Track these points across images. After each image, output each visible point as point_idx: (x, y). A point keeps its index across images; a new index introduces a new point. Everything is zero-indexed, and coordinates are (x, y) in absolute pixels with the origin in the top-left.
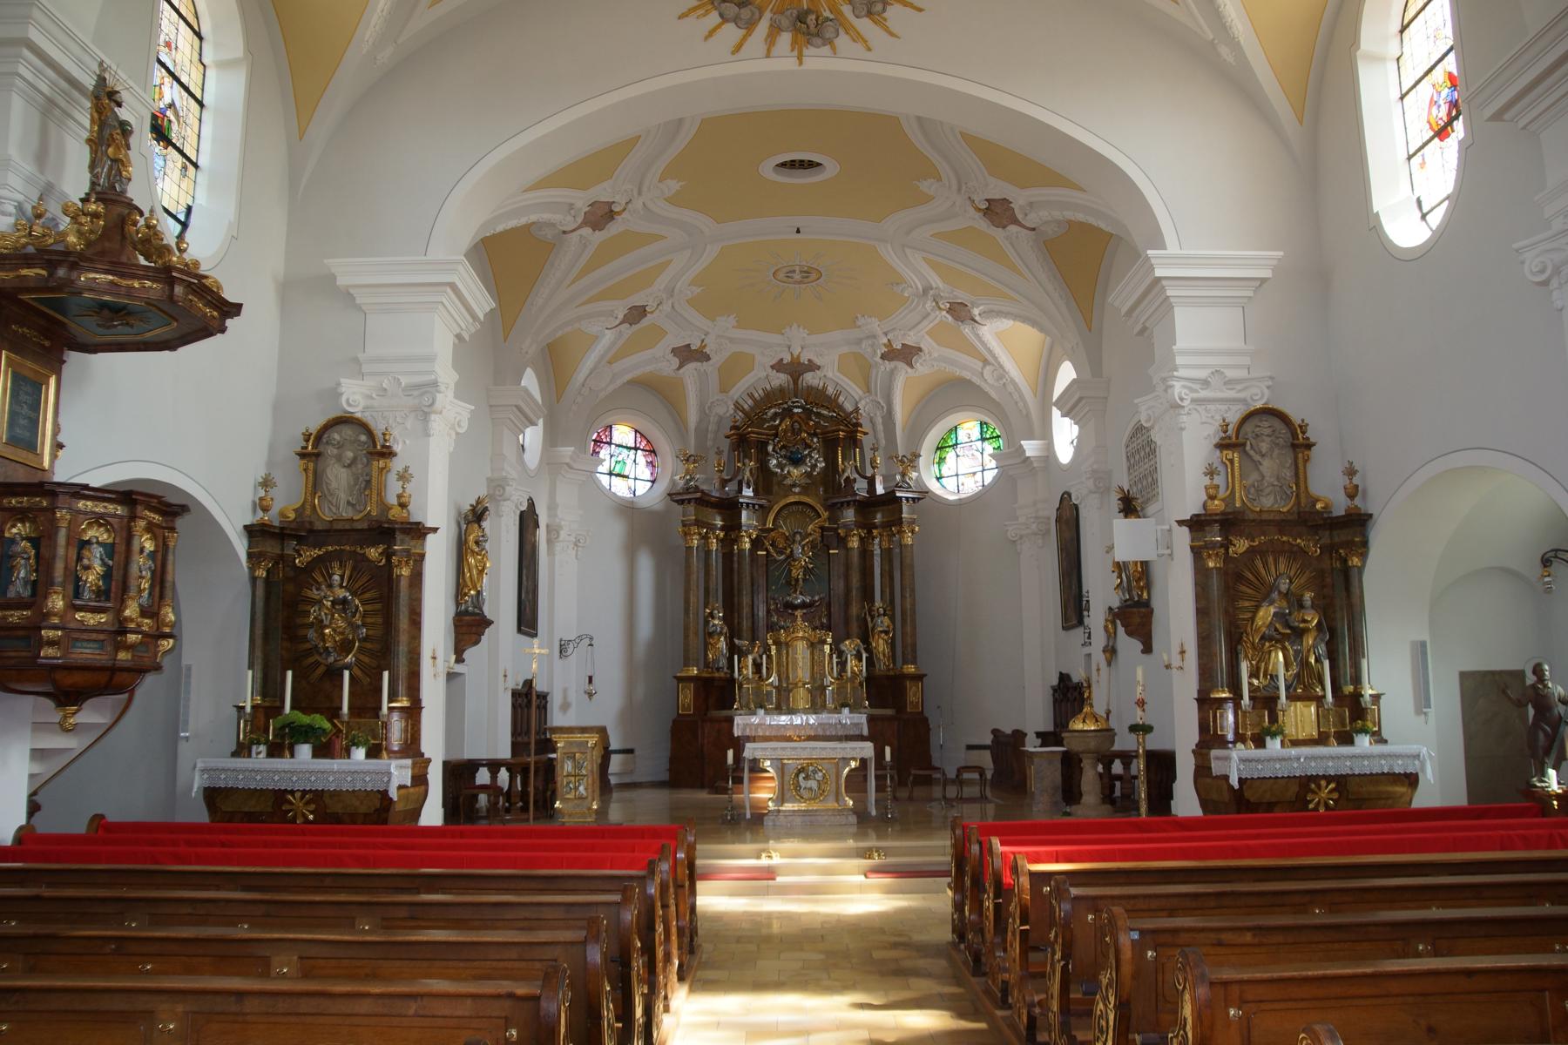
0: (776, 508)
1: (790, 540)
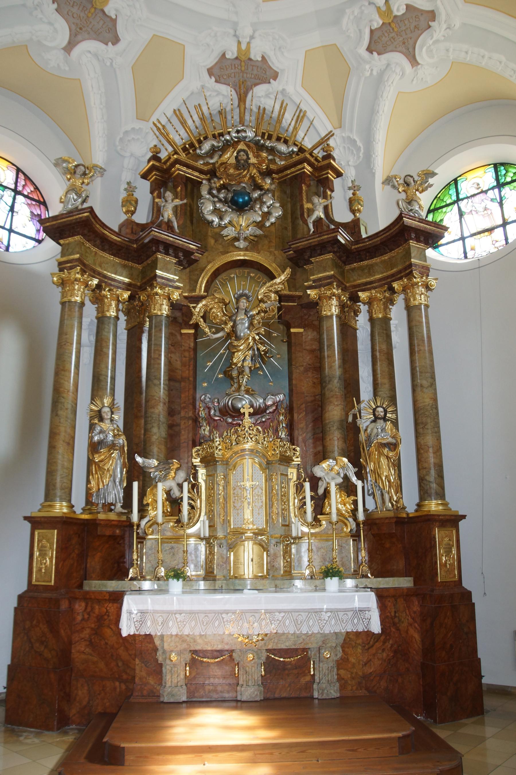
0: (211, 268)
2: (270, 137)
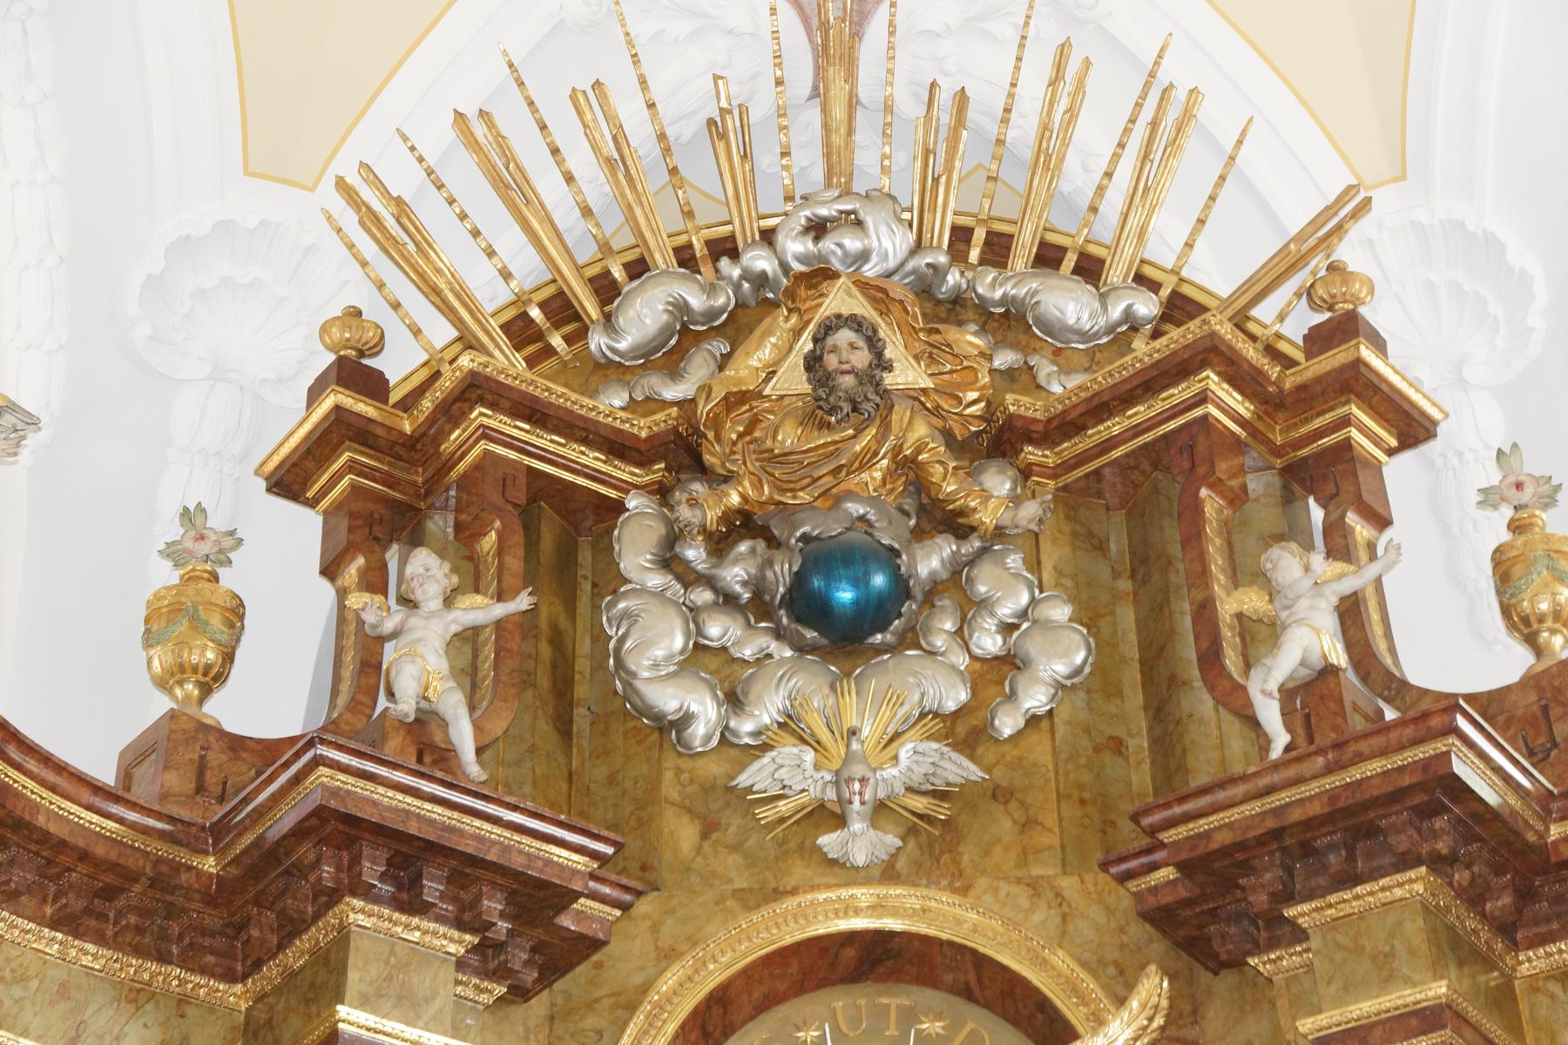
2: (998, 250)
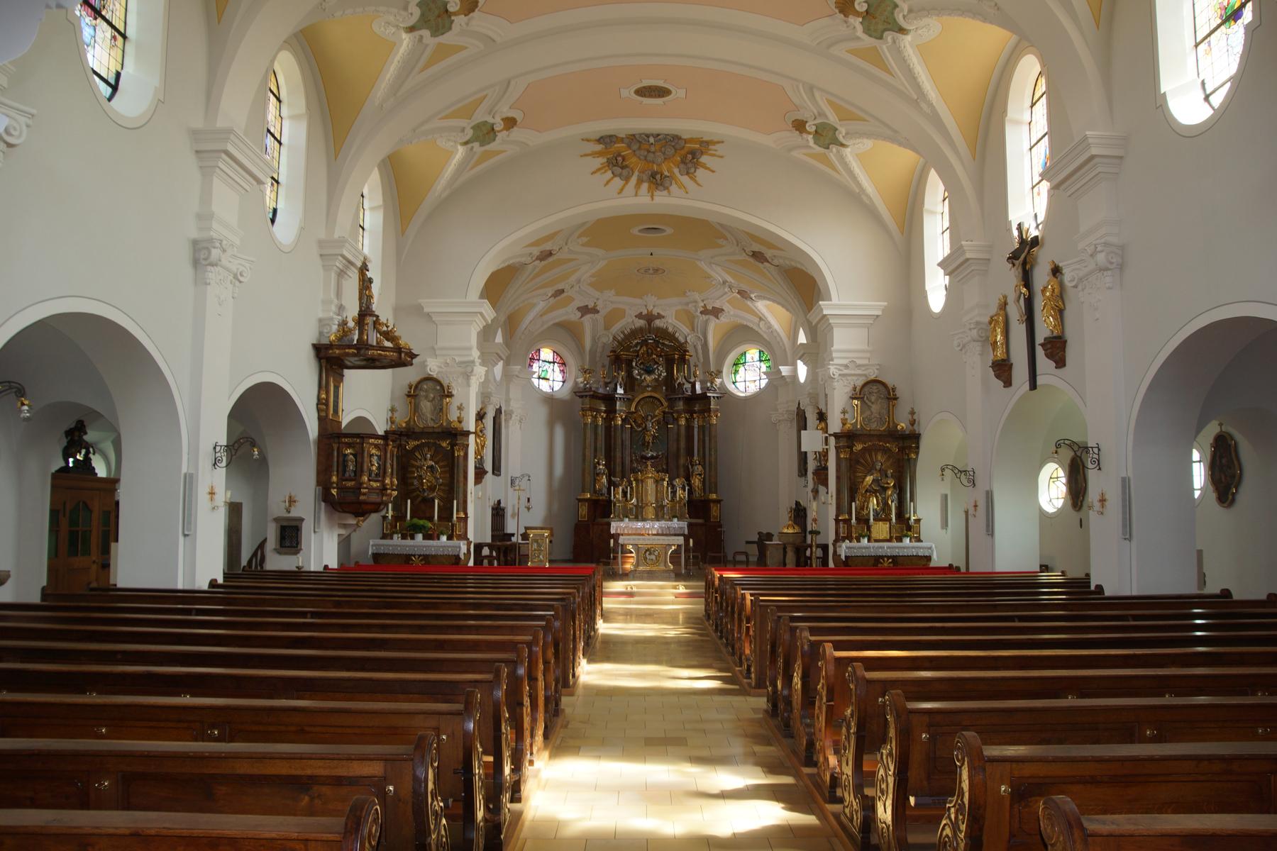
0: (637, 400)
1: (645, 419)
